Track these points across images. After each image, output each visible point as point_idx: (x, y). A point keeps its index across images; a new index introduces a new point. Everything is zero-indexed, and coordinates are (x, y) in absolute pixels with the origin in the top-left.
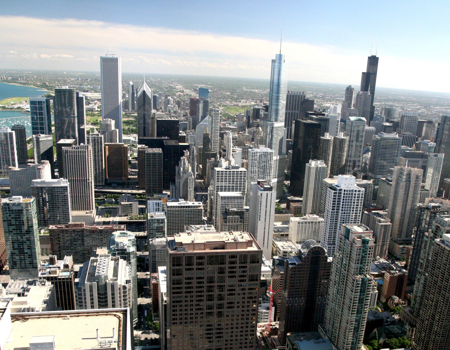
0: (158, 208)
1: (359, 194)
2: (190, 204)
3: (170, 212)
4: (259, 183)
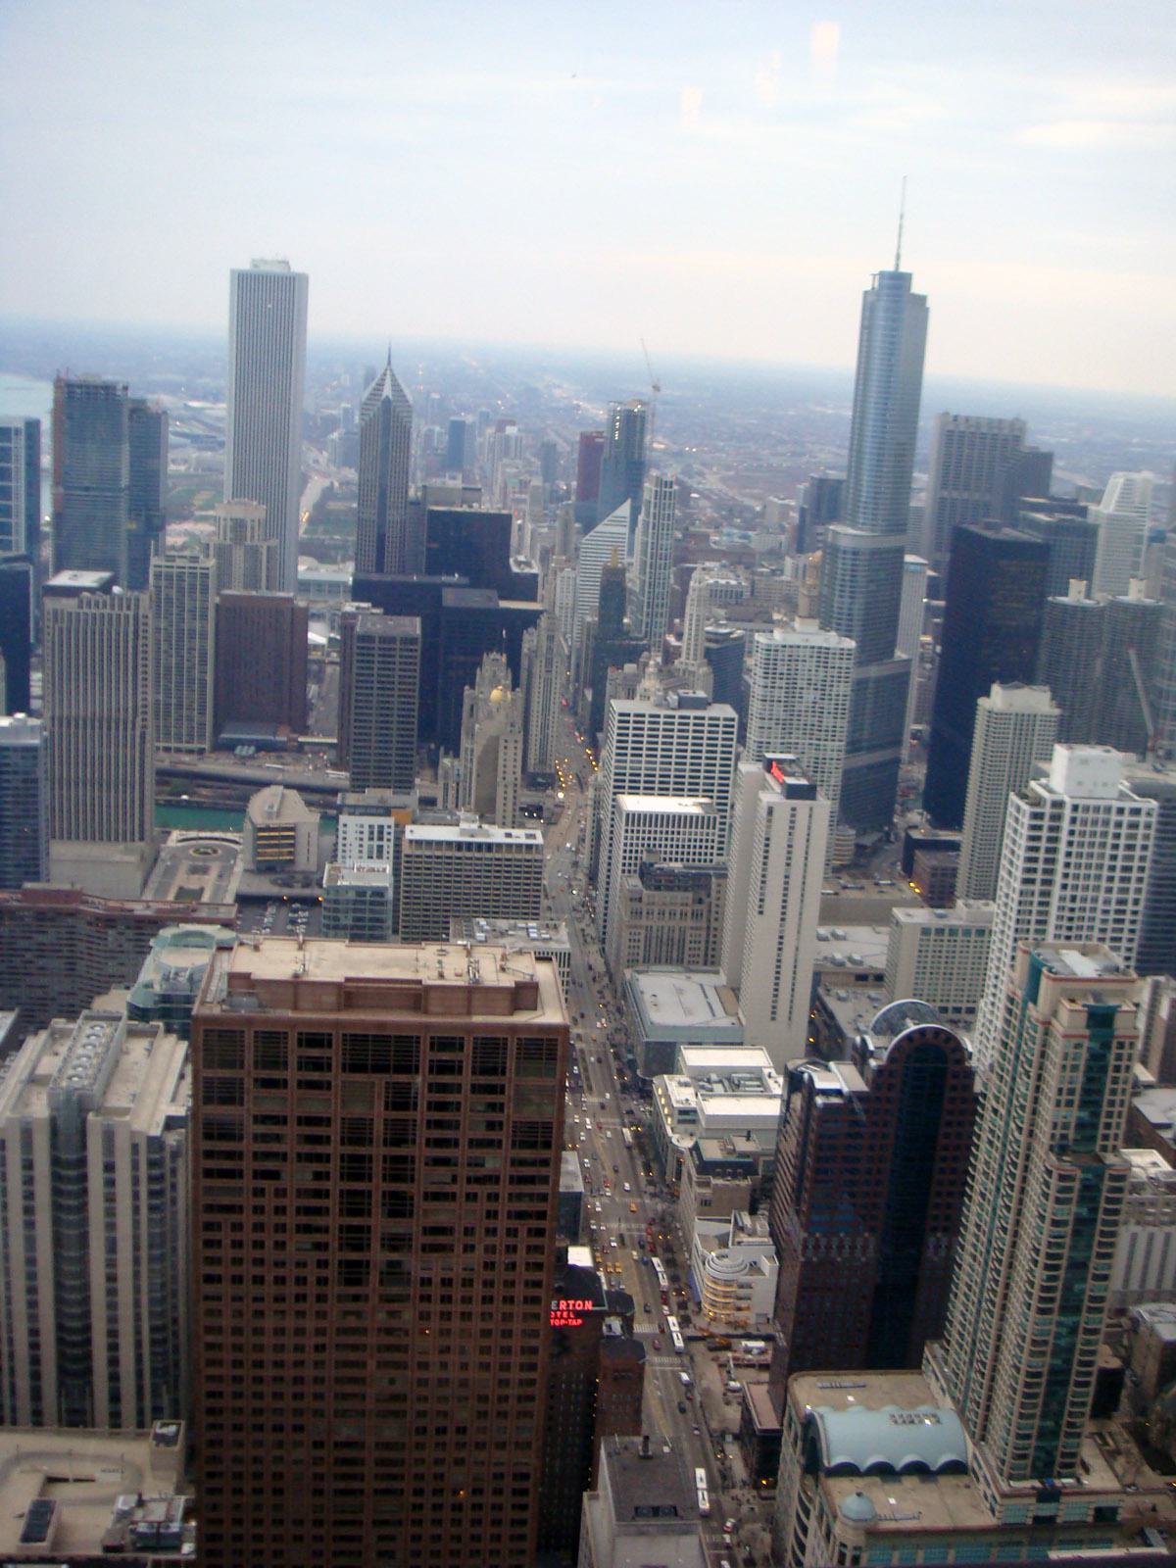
0: (380, 848)
1: (1134, 826)
2: (497, 835)
3: (409, 863)
4: (769, 765)
